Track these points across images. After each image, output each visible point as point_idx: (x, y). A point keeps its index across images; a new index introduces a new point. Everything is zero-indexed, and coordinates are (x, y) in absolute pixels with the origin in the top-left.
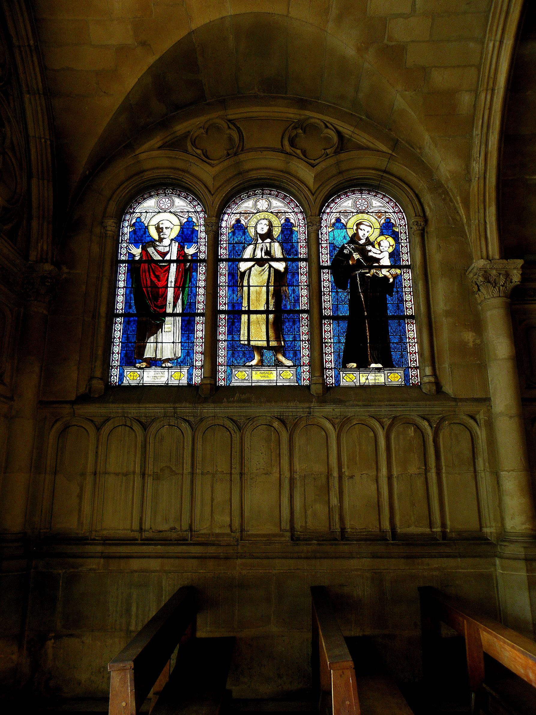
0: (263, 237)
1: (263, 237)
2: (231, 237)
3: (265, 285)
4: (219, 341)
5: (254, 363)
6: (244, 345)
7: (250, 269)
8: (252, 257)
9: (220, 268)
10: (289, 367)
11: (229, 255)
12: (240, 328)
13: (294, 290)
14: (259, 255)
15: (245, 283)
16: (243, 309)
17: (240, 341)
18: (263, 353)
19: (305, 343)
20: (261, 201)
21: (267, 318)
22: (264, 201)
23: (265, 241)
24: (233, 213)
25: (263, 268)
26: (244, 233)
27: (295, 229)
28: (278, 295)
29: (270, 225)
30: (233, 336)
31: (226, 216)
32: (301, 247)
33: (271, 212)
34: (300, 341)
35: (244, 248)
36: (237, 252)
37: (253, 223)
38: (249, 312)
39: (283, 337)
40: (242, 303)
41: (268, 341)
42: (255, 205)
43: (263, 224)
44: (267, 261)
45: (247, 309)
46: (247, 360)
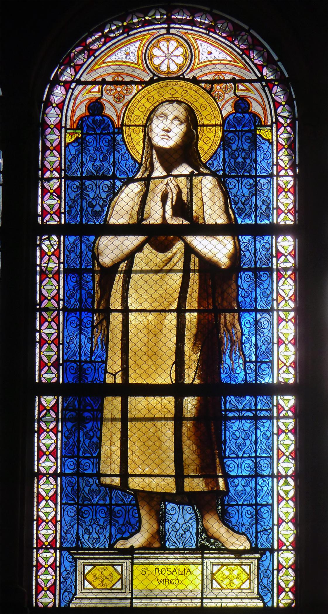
0: (170, 158)
1: (170, 158)
2: (74, 158)
3: (174, 306)
4: (40, 475)
5: (138, 540)
6: (111, 488)
7: (130, 257)
8: (133, 221)
9: (43, 253)
10: (238, 554)
11: (68, 213)
12: (100, 439)
13: (257, 322)
14: (155, 214)
15: (116, 303)
16: (109, 380)
17: (99, 475)
18: (164, 511)
19: (287, 484)
20: (163, 45)
21: (179, 406)
22: (173, 44)
23: (175, 172)
24: (79, 82)
25: (169, 254)
26: (113, 146)
27: (265, 133)
28: (211, 342)
29: (191, 120)
30: (78, 463)
31: (59, 91)
32: (280, 190)
33: (195, 81)
34: (272, 476)
35: (114, 193)
36: (93, 207)
37: (138, 115)
38: (127, 390)
39: (223, 466)
40: (105, 362)
41: (179, 476)
42: (146, 56)
43: (171, 117)
44: (180, 232)
45: (119, 381)
46: (120, 531)
